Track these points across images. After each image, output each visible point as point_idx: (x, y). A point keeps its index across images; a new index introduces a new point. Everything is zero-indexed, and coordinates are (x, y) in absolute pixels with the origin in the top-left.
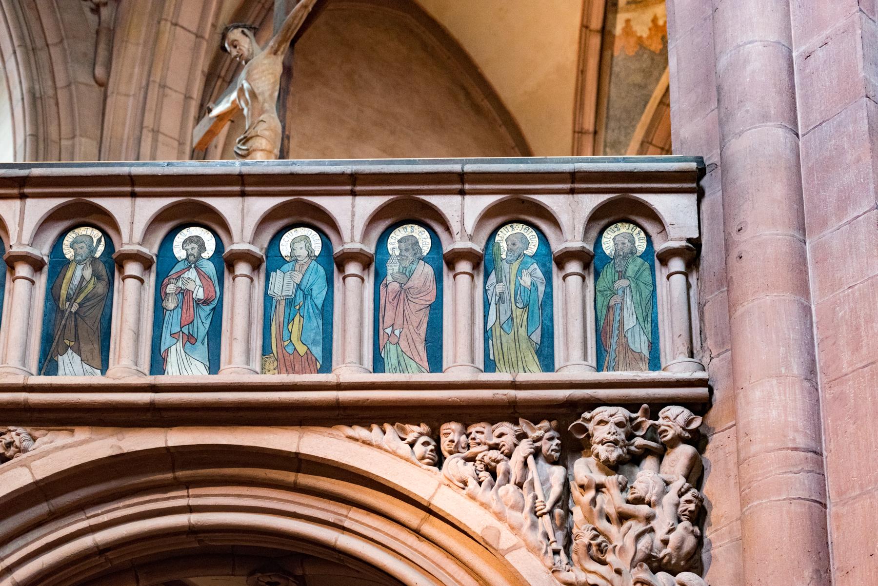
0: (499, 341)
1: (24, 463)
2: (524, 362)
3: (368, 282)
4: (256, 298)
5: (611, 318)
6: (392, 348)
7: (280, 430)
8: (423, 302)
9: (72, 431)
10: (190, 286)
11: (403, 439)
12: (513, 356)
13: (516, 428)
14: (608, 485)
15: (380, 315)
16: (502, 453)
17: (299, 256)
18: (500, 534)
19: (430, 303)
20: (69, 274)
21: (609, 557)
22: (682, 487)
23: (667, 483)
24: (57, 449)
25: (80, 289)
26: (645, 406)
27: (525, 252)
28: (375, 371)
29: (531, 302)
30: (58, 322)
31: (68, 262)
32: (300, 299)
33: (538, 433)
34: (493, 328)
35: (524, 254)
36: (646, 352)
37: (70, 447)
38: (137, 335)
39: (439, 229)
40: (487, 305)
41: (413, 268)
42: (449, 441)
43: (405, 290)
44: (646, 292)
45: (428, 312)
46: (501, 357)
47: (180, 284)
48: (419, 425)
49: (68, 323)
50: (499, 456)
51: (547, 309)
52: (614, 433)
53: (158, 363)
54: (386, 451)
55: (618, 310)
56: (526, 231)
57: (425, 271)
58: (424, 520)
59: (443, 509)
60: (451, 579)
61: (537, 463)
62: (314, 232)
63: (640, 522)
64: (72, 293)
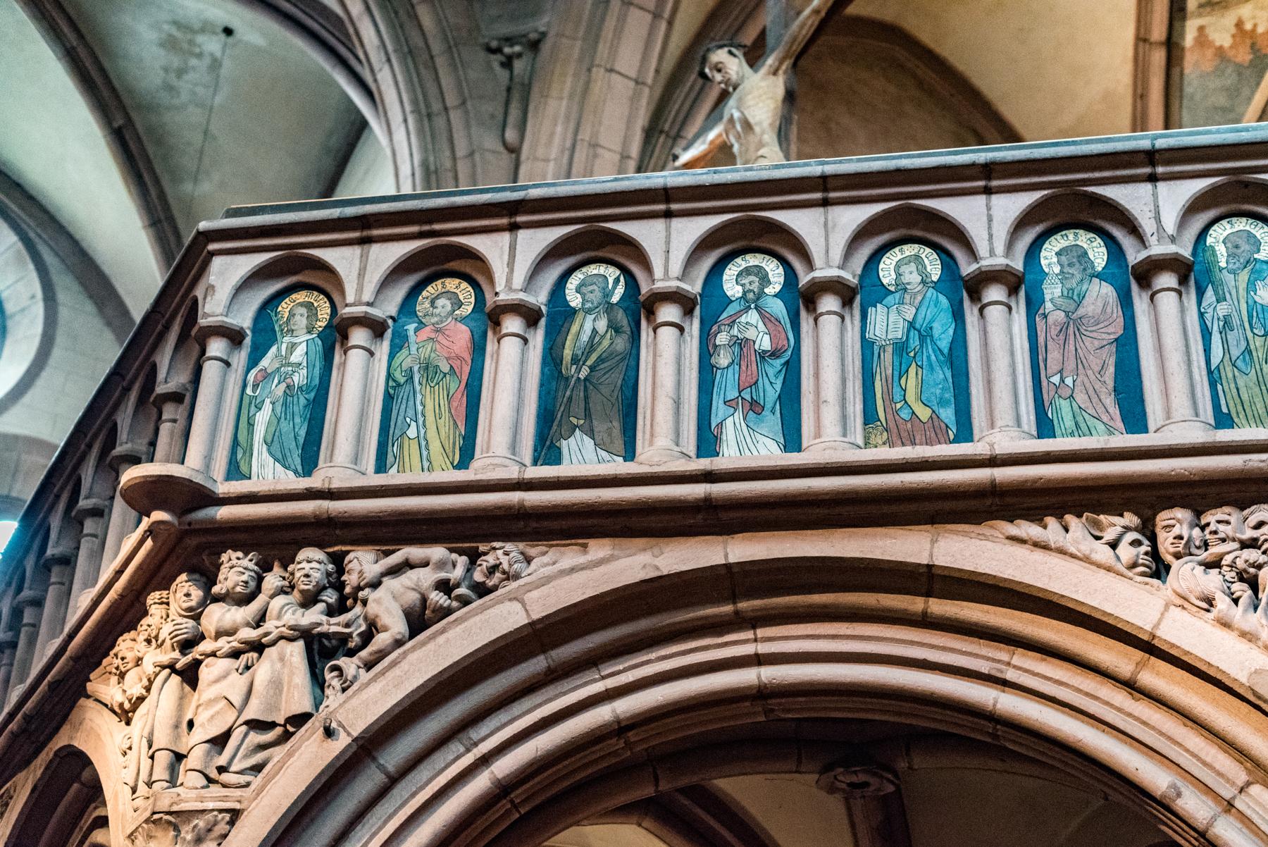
0: (1233, 386)
1: (512, 596)
3: (1018, 312)
4: (850, 344)
6: (1064, 405)
7: (901, 532)
8: (1104, 336)
9: (585, 546)
10: (751, 334)
11: (1098, 538)
15: (1040, 357)
17: (908, 284)
19: (1116, 337)
20: (574, 328)
24: (563, 573)
25: (591, 346)
27: (1256, 256)
28: (1040, 436)
30: (560, 393)
31: (574, 312)
32: (914, 342)
34: (1221, 367)
35: (1255, 259)
37: (582, 569)
38: (677, 403)
39: (1118, 233)
40: (1206, 334)
41: (1084, 288)
42: (1175, 538)
46: (1240, 408)
47: (735, 331)
48: (1122, 515)
53: (708, 441)
54: (1073, 556)
56: (1253, 226)
57: (1101, 294)
58: (1140, 665)
60: (1194, 760)
62: (928, 250)
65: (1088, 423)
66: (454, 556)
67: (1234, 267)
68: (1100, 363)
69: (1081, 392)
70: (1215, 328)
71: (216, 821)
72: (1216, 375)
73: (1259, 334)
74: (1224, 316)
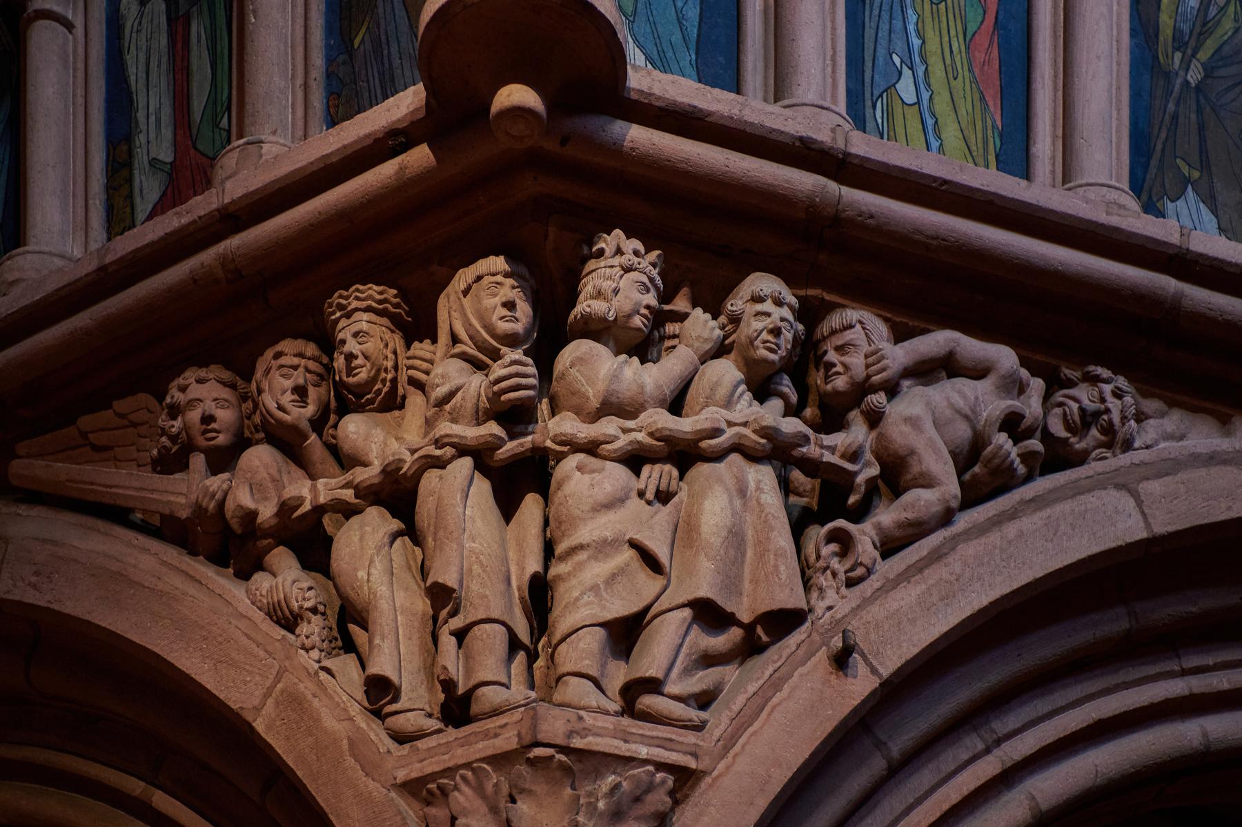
49: (1181, 110)
64: (1186, 28)
66: (1024, 373)
71: (651, 783)
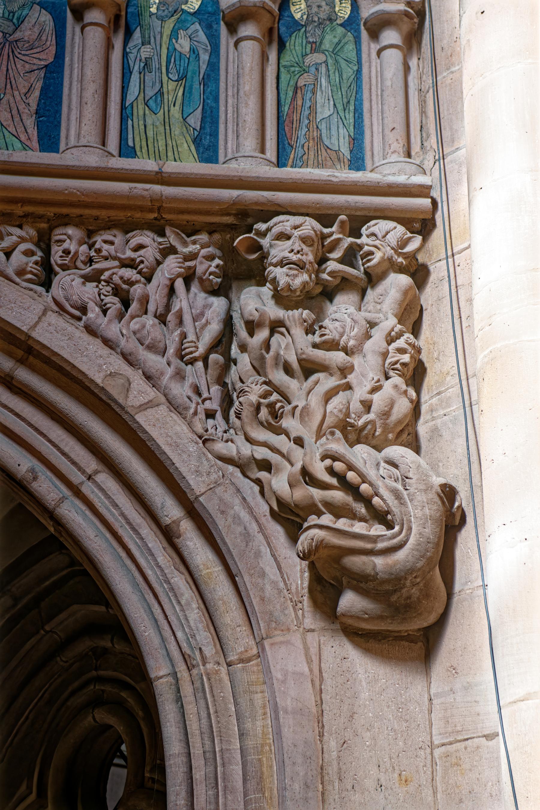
0: (141, 122)
2: (175, 153)
5: (300, 102)
8: (35, 61)
12: (162, 143)
13: (160, 240)
14: (288, 323)
16: (140, 272)
18: (130, 384)
19: (46, 64)
21: (287, 423)
22: (392, 330)
23: (372, 324)
26: (343, 217)
29: (189, 74)
33: (192, 248)
34: (135, 105)
35: (182, 10)
36: (345, 151)
41: (25, 13)
43: (11, 43)
44: (349, 72)
45: (43, 75)
50: (134, 276)
51: (212, 86)
52: (298, 252)
55: (309, 92)
59: (49, 346)
60: (55, 450)
61: (188, 289)
63: (331, 375)
65: (7, 140)
67: (163, 14)
68: (27, 85)
69: (6, 110)
70: (136, 68)
72: (128, 111)
73: (173, 79)
74: (146, 58)
